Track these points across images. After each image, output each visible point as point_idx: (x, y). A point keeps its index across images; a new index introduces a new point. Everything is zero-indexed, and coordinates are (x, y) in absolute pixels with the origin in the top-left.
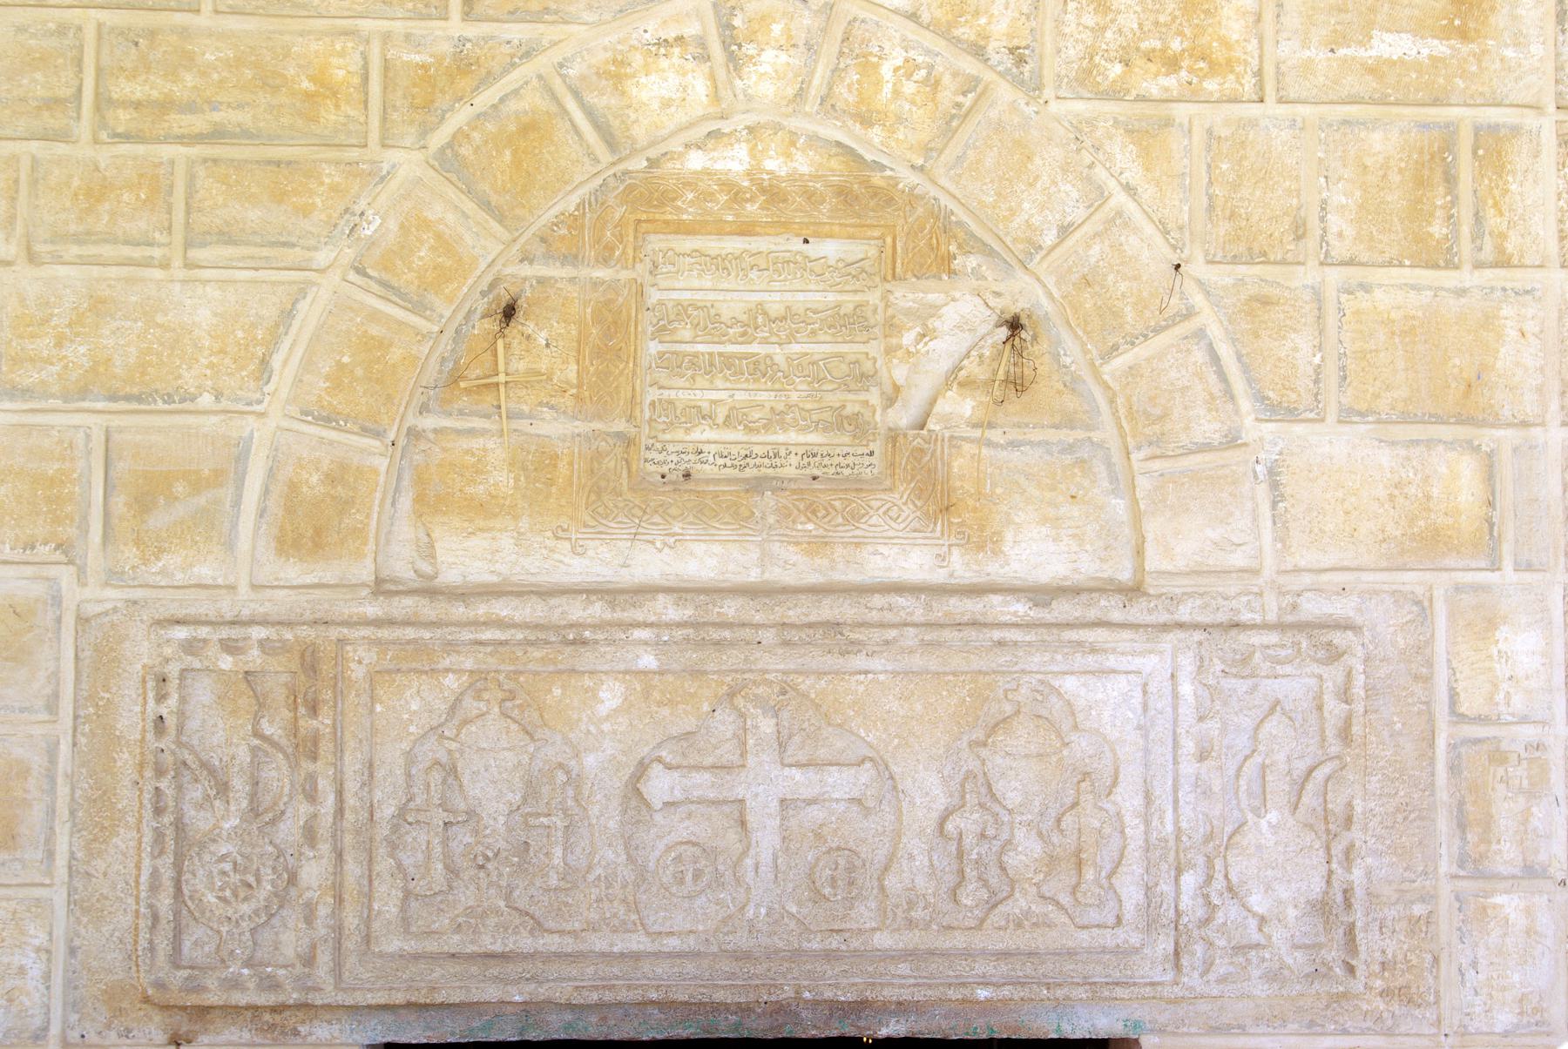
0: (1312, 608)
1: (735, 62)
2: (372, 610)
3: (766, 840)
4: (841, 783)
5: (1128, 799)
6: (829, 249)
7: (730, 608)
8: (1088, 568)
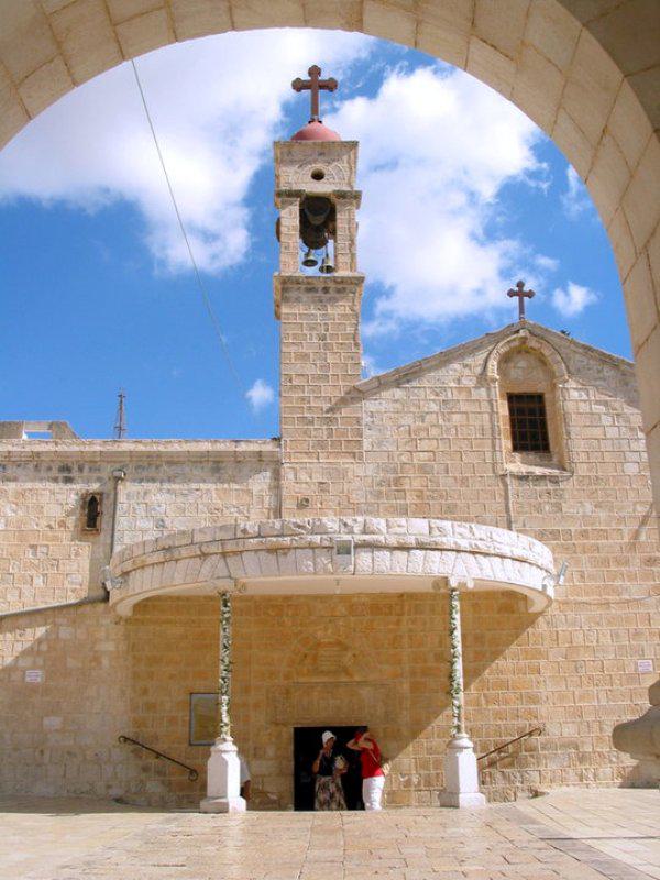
4: (338, 701)
6: (335, 649)
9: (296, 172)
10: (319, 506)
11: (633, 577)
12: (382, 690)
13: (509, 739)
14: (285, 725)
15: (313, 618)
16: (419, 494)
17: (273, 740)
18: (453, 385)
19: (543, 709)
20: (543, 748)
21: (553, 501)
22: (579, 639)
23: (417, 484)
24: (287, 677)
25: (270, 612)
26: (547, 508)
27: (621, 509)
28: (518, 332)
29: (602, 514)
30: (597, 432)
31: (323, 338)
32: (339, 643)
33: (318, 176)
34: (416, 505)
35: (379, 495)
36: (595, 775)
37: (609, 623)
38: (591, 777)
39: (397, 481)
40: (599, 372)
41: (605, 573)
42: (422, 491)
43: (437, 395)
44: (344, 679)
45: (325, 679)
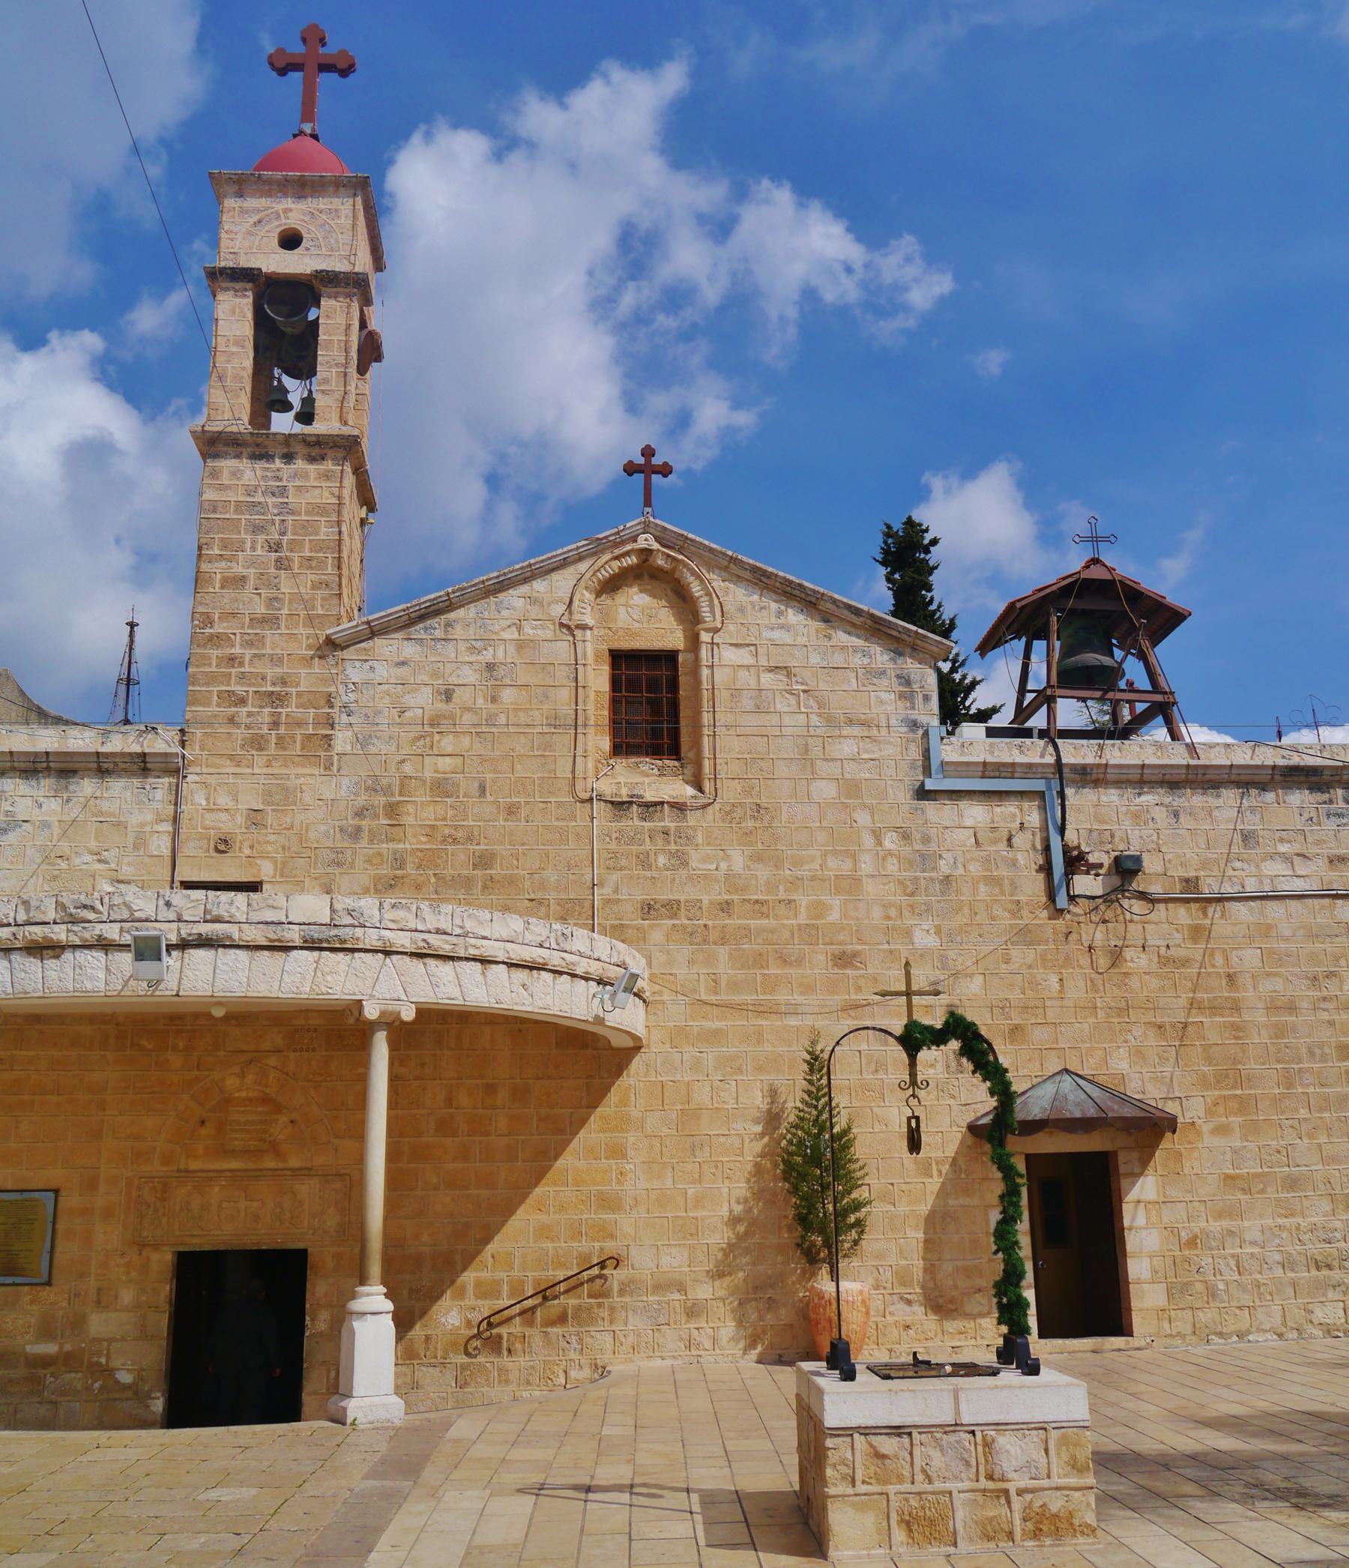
0: (343, 1171)
1: (244, 1077)
2: (176, 1175)
3: (242, 1214)
4: (256, 1204)
5: (306, 1206)
6: (260, 1109)
7: (239, 1174)
8: (304, 1165)
9: (249, 233)
10: (247, 851)
11: (808, 989)
12: (338, 1185)
13: (561, 1275)
14: (156, 1247)
15: (222, 1053)
16: (428, 830)
17: (133, 1274)
19: (625, 1223)
20: (622, 1292)
21: (673, 847)
22: (702, 1095)
23: (429, 815)
24: (166, 1160)
25: (144, 1043)
26: (662, 860)
27: (798, 863)
28: (634, 539)
29: (763, 873)
31: (272, 548)
32: (265, 1100)
33: (291, 241)
36: (714, 1341)
37: (759, 1069)
38: (708, 1345)
39: (392, 810)
40: (780, 614)
42: (433, 827)
44: (270, 1163)
45: (235, 1165)
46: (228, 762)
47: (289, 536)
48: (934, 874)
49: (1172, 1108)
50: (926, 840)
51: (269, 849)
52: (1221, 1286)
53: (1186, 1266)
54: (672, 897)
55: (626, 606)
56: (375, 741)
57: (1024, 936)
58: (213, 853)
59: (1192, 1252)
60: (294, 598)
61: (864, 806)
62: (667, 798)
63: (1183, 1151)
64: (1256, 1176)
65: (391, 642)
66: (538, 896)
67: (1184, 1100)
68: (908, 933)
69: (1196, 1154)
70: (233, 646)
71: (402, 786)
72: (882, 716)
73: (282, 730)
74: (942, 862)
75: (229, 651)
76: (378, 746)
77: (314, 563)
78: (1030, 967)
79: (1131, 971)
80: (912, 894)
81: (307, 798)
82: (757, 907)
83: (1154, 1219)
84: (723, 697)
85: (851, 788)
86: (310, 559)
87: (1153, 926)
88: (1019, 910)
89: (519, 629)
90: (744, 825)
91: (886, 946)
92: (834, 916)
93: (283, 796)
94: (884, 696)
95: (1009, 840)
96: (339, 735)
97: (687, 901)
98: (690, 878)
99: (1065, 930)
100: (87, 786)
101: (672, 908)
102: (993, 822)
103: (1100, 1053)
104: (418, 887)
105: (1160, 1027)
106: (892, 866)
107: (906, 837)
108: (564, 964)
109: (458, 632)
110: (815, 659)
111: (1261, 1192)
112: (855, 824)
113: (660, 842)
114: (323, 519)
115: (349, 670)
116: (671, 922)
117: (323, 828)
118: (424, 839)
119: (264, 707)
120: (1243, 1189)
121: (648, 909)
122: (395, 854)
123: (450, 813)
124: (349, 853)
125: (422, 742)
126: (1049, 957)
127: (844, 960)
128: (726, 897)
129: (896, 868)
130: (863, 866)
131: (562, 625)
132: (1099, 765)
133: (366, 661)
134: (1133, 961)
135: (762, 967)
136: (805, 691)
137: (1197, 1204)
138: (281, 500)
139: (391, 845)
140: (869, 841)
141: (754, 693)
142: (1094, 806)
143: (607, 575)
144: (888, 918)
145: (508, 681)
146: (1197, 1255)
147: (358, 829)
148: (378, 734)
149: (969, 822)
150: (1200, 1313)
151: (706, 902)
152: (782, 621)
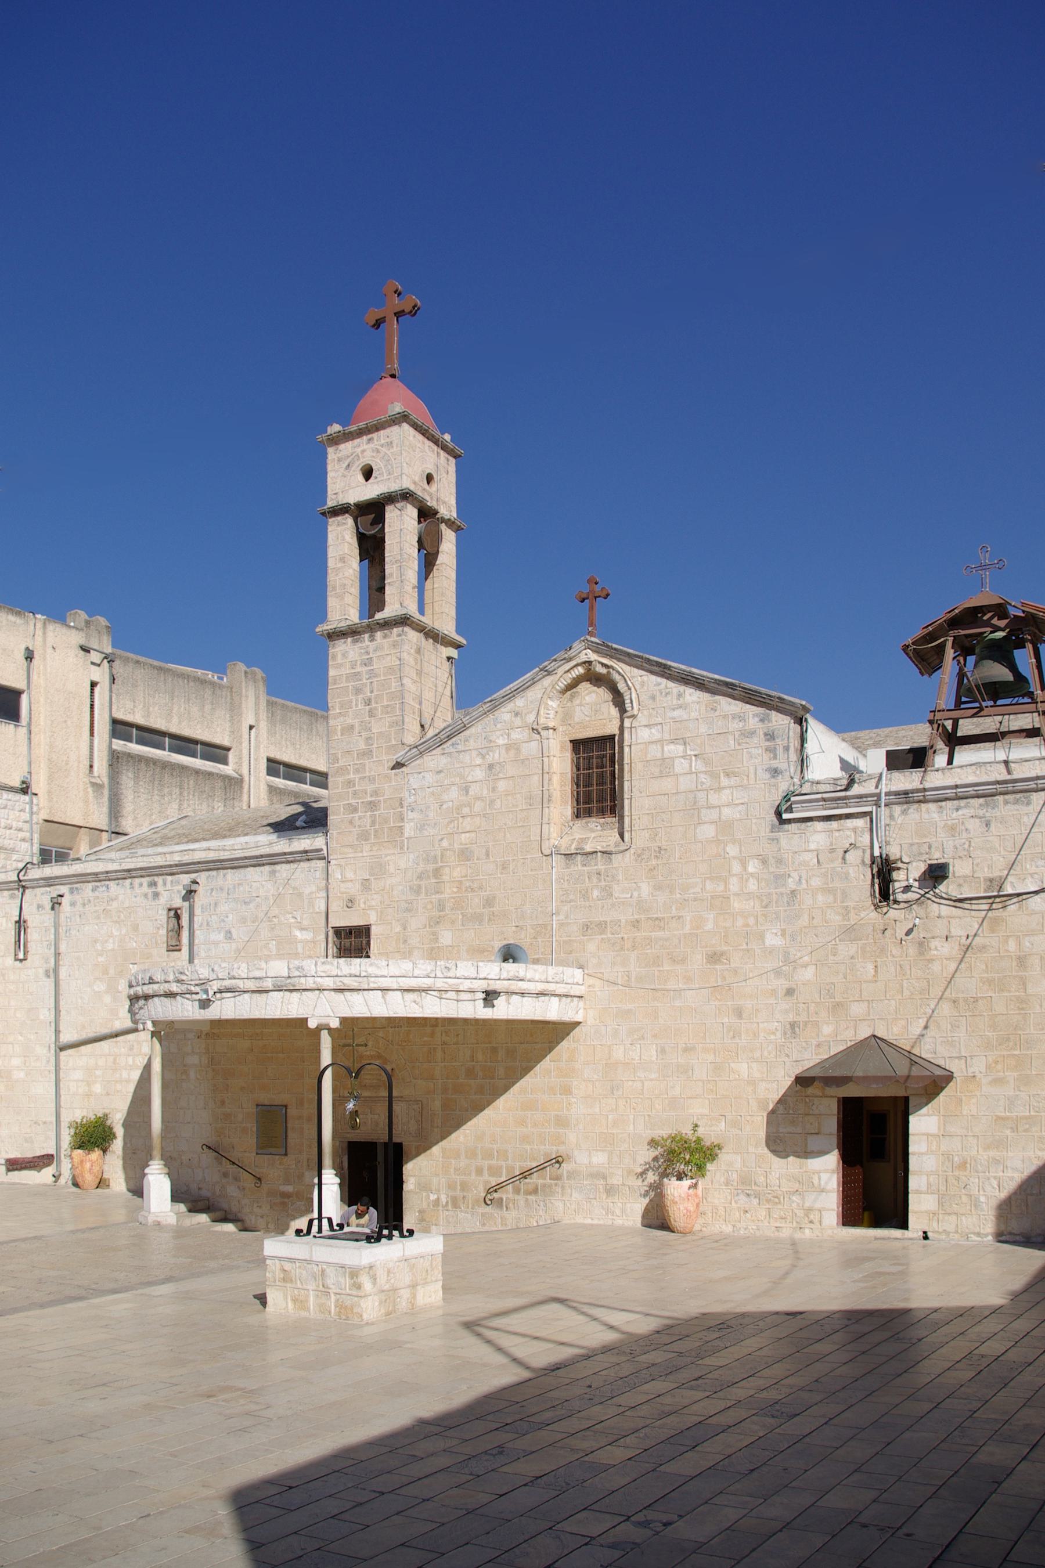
10: (362, 906)
18: (501, 741)
21: (603, 883)
23: (457, 873)
26: (596, 893)
30: (667, 784)
31: (368, 702)
34: (454, 898)
35: (417, 891)
39: (437, 873)
41: (656, 973)
42: (461, 882)
43: (483, 757)
46: (351, 850)
47: (375, 693)
48: (783, 890)
49: (954, 1066)
50: (780, 861)
51: (374, 904)
52: (982, 1199)
53: (956, 1183)
54: (602, 919)
55: (581, 705)
56: (426, 827)
57: (850, 933)
58: (346, 909)
59: (961, 1173)
60: (381, 734)
61: (734, 842)
62: (599, 848)
63: (964, 1098)
64: (1026, 1118)
65: (433, 757)
66: (521, 923)
67: (969, 1058)
68: (762, 937)
69: (974, 1100)
70: (349, 773)
71: (442, 856)
72: (751, 768)
73: (377, 827)
74: (790, 880)
75: (348, 777)
76: (430, 831)
77: (389, 709)
78: (852, 958)
79: (934, 958)
80: (766, 907)
81: (392, 869)
82: (657, 922)
83: (934, 1148)
84: (638, 767)
85: (725, 827)
86: (388, 706)
87: (957, 920)
88: (847, 914)
89: (509, 735)
90: (650, 863)
91: (745, 947)
92: (710, 926)
93: (378, 869)
94: (753, 751)
95: (844, 858)
96: (407, 825)
97: (611, 921)
98: (613, 905)
99: (882, 928)
100: (283, 869)
101: (602, 926)
102: (831, 844)
103: (903, 1022)
104: (453, 922)
105: (954, 1002)
106: (752, 886)
107: (764, 862)
108: (446, 986)
109: (472, 744)
110: (703, 729)
111: (1026, 1131)
112: (727, 856)
113: (595, 880)
114: (392, 677)
115: (412, 780)
116: (600, 937)
117: (401, 887)
118: (455, 890)
119: (366, 812)
120: (1012, 1128)
121: (586, 927)
122: (439, 901)
123: (469, 871)
124: (415, 902)
125: (452, 825)
126: (868, 949)
127: (714, 958)
128: (636, 917)
129: (756, 888)
130: (731, 887)
131: (533, 729)
132: (918, 791)
133: (420, 773)
134: (936, 949)
135: (659, 966)
136: (695, 756)
137: (970, 1139)
138: (369, 668)
139: (438, 896)
140: (736, 868)
141: (658, 763)
142: (916, 824)
143: (563, 686)
144: (747, 925)
145: (501, 775)
146: (966, 1176)
147: (419, 886)
148: (428, 822)
149: (813, 846)
150: (963, 1218)
151: (623, 921)
152: (681, 701)
